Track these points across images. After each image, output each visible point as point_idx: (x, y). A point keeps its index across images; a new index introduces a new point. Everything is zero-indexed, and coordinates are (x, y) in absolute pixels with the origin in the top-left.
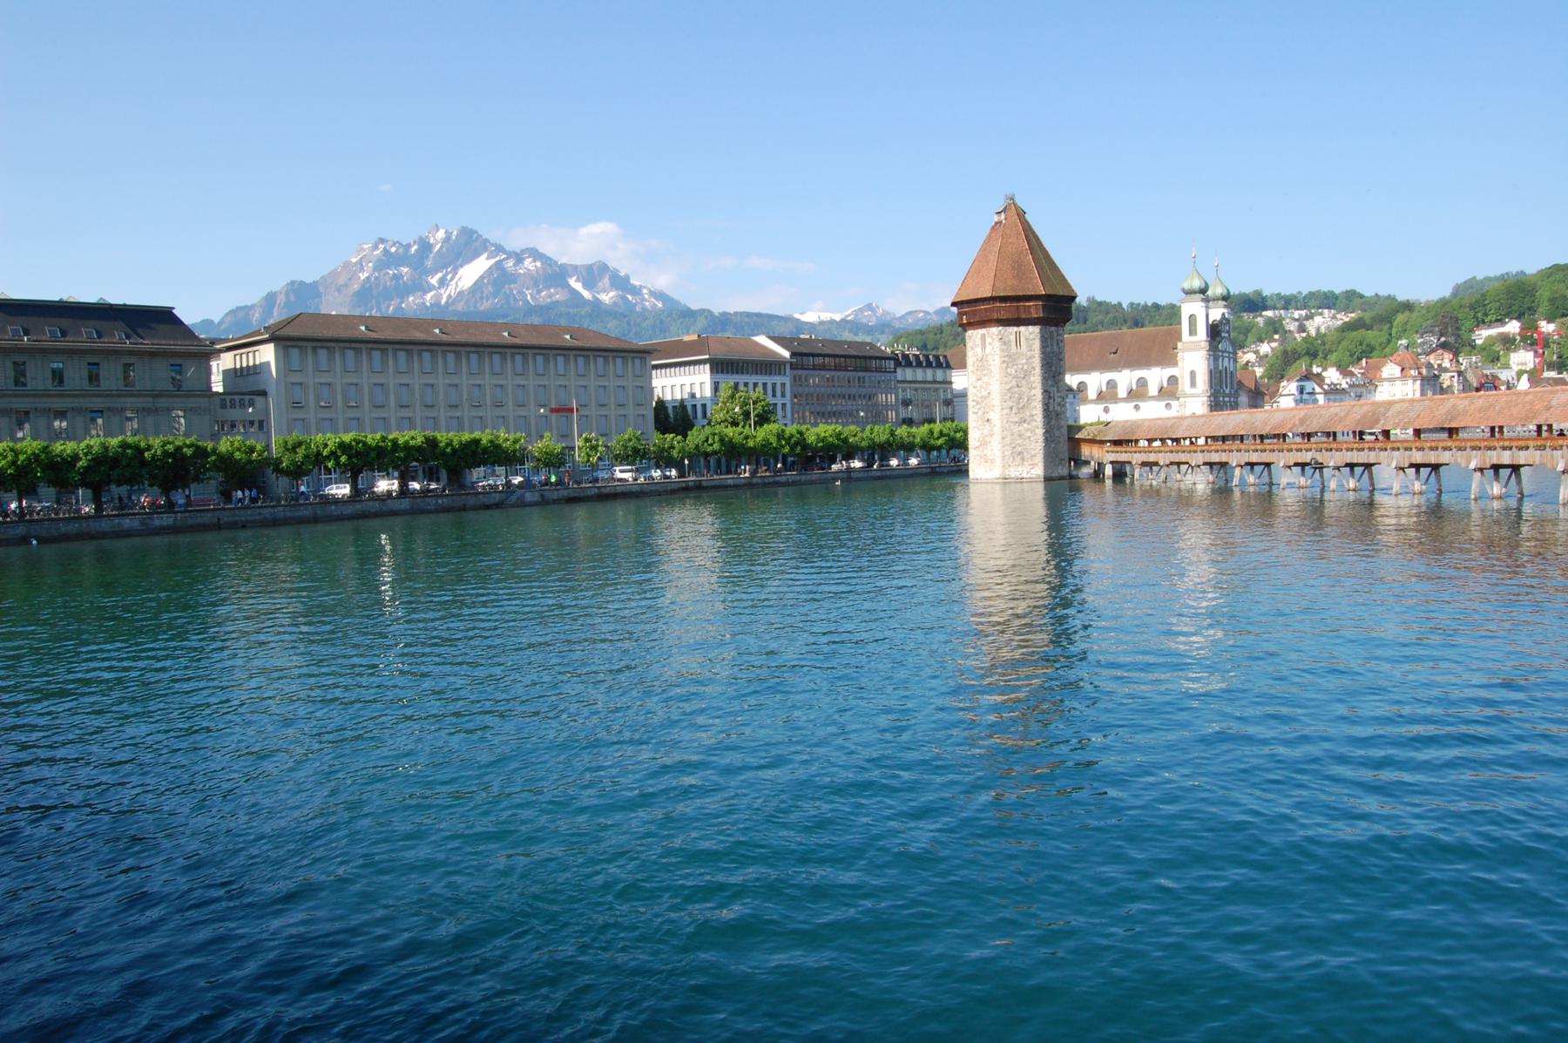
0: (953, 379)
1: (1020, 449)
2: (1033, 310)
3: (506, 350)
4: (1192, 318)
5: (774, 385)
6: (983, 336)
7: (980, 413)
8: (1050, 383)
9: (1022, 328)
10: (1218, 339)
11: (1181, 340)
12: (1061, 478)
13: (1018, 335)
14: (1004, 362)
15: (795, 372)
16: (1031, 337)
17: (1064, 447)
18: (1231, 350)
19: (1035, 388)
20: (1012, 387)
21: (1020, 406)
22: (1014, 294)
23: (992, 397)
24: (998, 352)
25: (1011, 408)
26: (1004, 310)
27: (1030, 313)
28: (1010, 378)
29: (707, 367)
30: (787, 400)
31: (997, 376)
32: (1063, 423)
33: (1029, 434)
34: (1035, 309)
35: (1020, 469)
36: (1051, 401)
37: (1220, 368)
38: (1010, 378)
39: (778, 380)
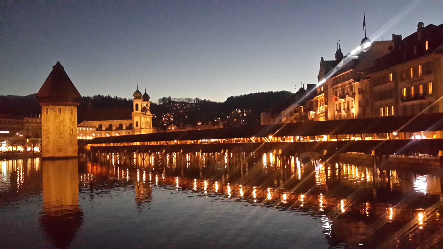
4: (137, 105)
8: (71, 125)
9: (61, 107)
11: (133, 111)
14: (54, 118)
20: (57, 126)
21: (60, 133)
28: (56, 123)
33: (63, 142)
37: (146, 120)
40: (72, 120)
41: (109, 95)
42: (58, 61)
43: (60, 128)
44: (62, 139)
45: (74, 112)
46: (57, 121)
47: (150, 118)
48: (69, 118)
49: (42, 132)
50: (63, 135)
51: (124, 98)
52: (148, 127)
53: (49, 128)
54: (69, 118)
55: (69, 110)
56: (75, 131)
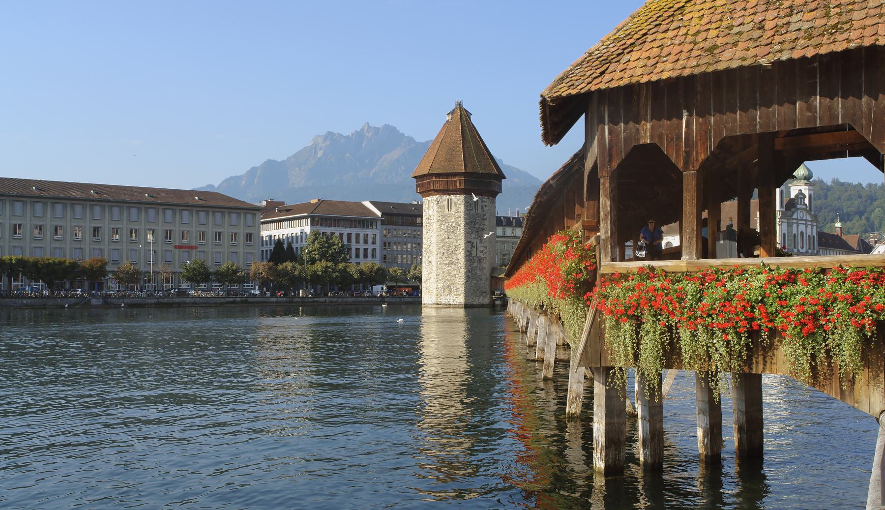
1: (449, 283)
2: (458, 184)
3: (159, 206)
5: (366, 236)
8: (473, 236)
9: (452, 197)
10: (793, 210)
12: (482, 306)
13: (450, 201)
14: (439, 220)
15: (385, 227)
17: (485, 284)
18: (809, 218)
20: (444, 239)
22: (443, 172)
24: (436, 213)
25: (443, 253)
26: (439, 184)
27: (455, 185)
28: (443, 232)
29: (309, 220)
30: (378, 246)
34: (459, 183)
35: (448, 297)
36: (474, 249)
37: (794, 231)
38: (443, 232)
39: (370, 232)
40: (475, 224)
41: (820, 178)
42: (459, 100)
43: (449, 244)
45: (482, 208)
47: (809, 227)
48: (468, 221)
49: (424, 250)
50: (455, 258)
51: (857, 183)
52: (802, 248)
54: (468, 221)
56: (482, 249)
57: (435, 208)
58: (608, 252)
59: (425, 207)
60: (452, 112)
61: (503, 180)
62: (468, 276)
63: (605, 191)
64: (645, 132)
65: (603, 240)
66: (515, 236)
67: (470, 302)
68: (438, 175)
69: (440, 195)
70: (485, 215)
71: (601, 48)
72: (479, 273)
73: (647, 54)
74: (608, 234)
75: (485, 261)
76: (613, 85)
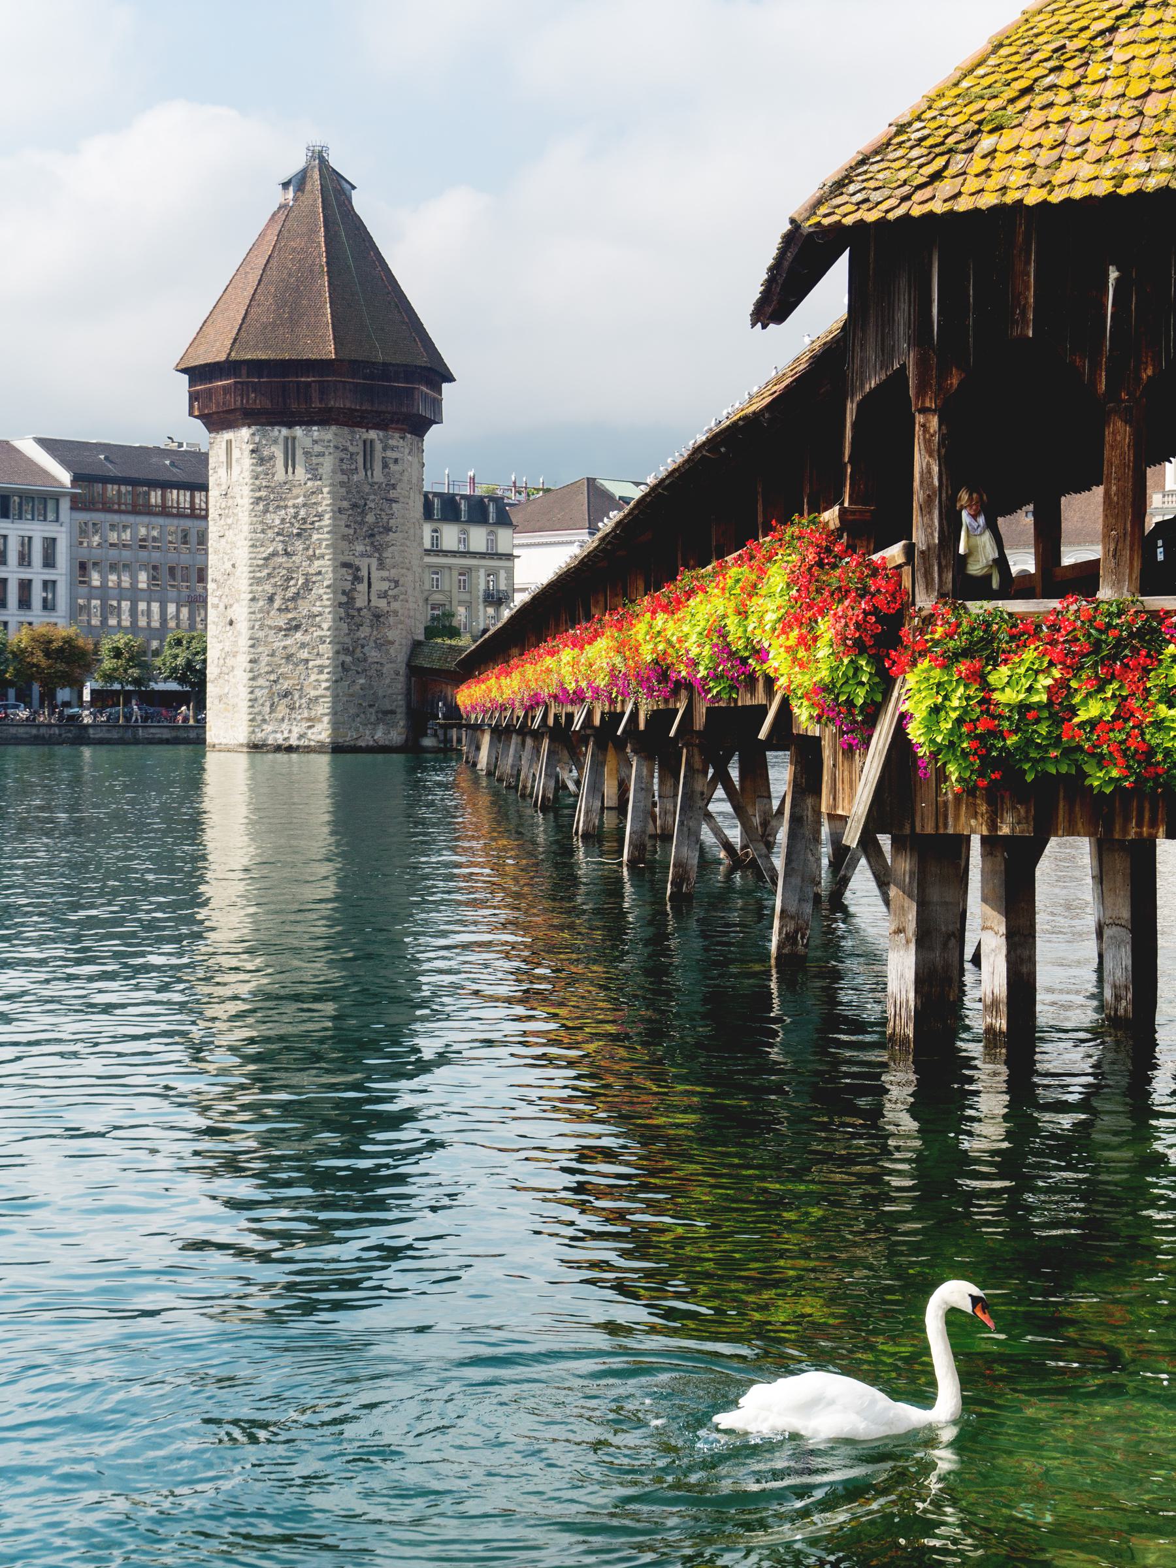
0: (516, 552)
1: (285, 685)
2: (315, 395)
6: (229, 442)
7: (222, 606)
8: (360, 548)
9: (298, 431)
14: (260, 498)
16: (318, 448)
19: (322, 557)
20: (274, 554)
21: (289, 594)
23: (238, 574)
25: (271, 599)
30: (61, 572)
31: (246, 528)
32: (391, 635)
33: (304, 654)
36: (362, 587)
39: (38, 531)
40: (363, 513)
42: (317, 139)
44: (298, 635)
45: (385, 466)
46: (277, 522)
48: (345, 504)
53: (233, 566)
54: (345, 504)
55: (345, 449)
56: (385, 586)
57: (244, 463)
58: (933, 579)
59: (217, 458)
60: (298, 182)
61: (445, 386)
62: (343, 664)
63: (927, 442)
64: (1024, 313)
65: (922, 552)
66: (468, 552)
67: (349, 737)
68: (257, 366)
69: (262, 424)
70: (394, 487)
71: (929, 114)
72: (373, 655)
73: (1035, 138)
74: (933, 537)
75: (391, 619)
76: (963, 205)
